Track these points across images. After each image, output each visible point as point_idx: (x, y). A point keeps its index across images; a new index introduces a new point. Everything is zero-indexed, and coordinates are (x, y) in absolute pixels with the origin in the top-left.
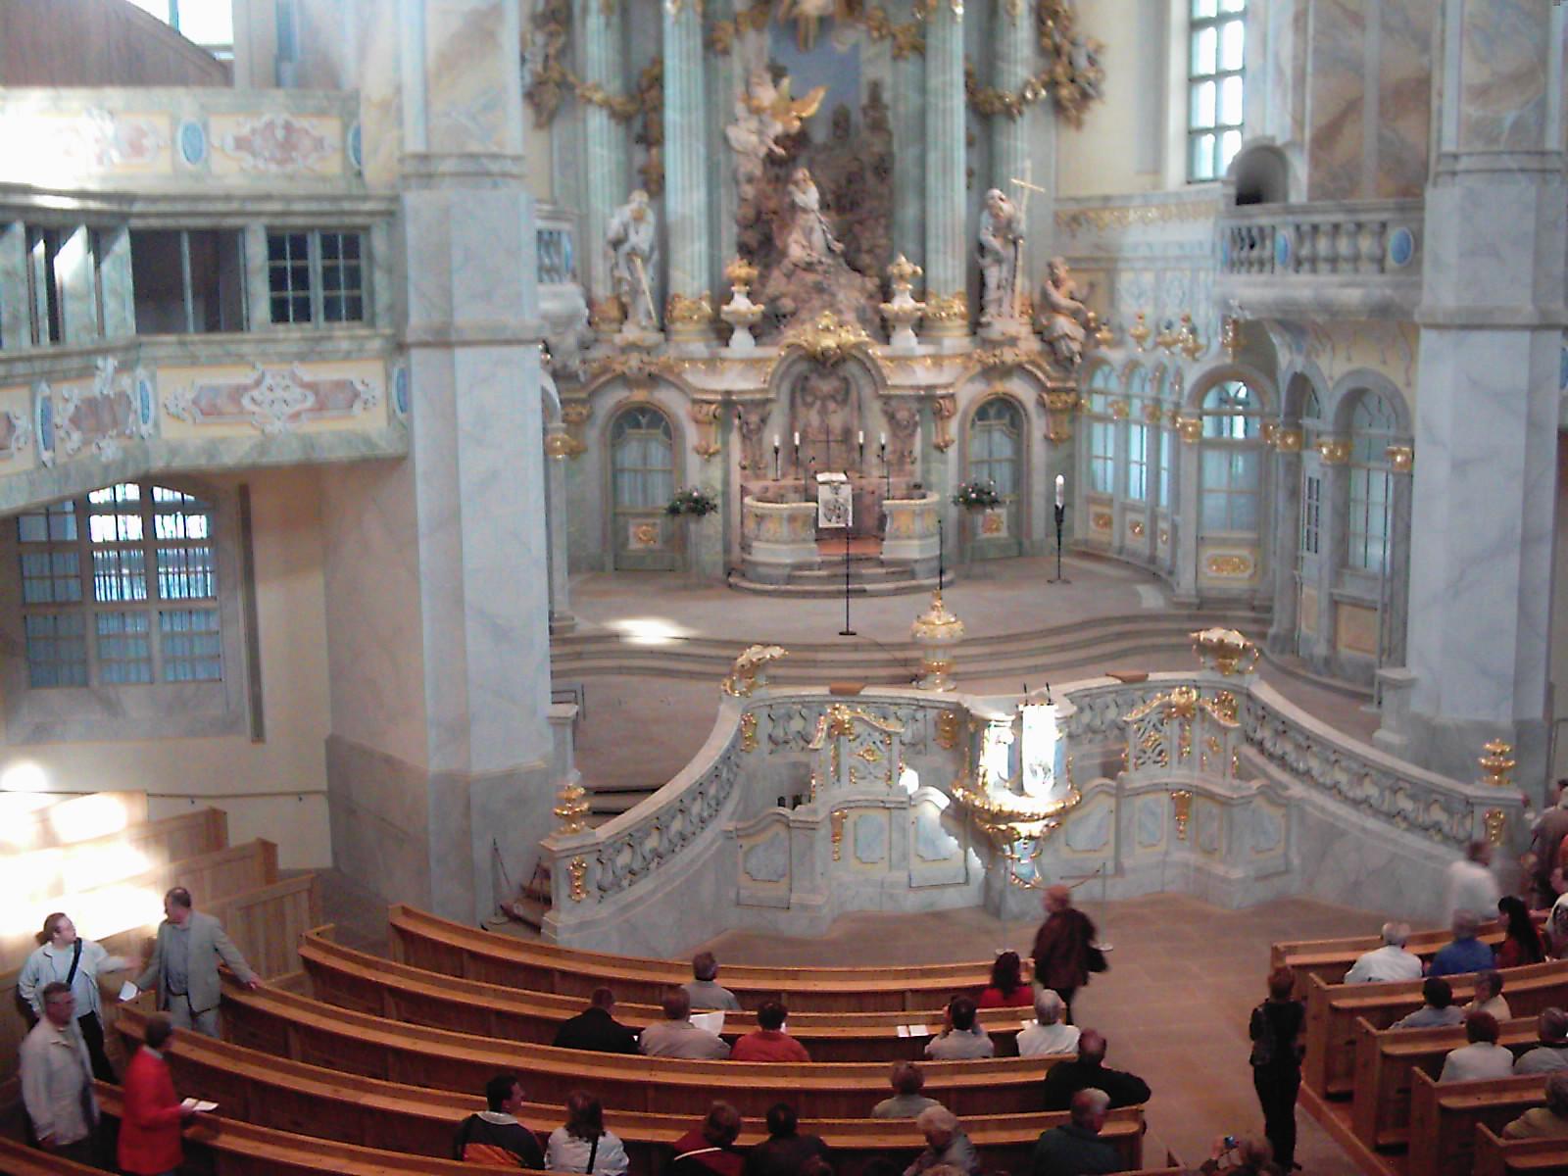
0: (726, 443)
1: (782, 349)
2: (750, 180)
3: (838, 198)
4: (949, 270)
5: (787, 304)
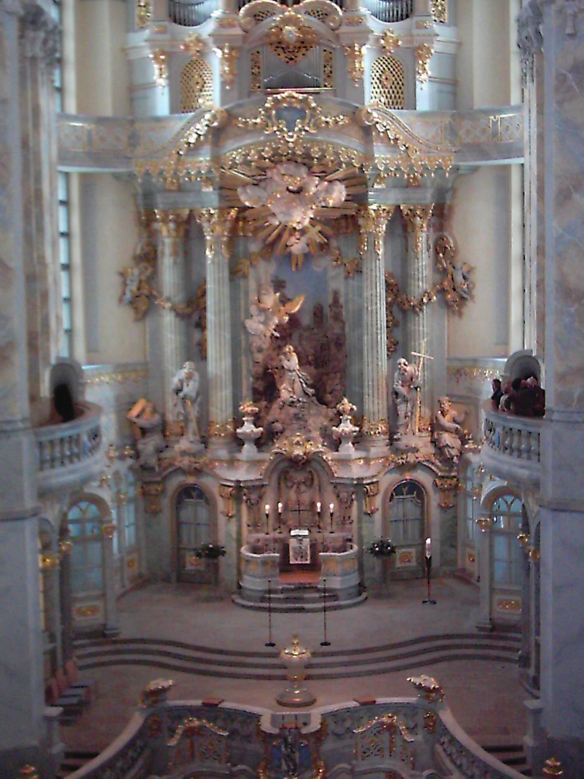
0: (239, 511)
1: (271, 456)
2: (260, 350)
3: (316, 359)
4: (376, 406)
5: (278, 426)
